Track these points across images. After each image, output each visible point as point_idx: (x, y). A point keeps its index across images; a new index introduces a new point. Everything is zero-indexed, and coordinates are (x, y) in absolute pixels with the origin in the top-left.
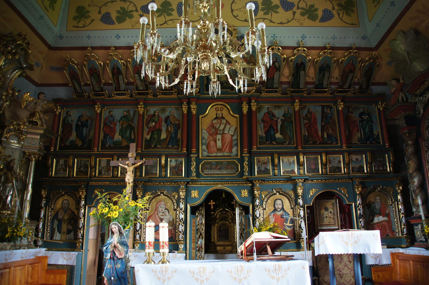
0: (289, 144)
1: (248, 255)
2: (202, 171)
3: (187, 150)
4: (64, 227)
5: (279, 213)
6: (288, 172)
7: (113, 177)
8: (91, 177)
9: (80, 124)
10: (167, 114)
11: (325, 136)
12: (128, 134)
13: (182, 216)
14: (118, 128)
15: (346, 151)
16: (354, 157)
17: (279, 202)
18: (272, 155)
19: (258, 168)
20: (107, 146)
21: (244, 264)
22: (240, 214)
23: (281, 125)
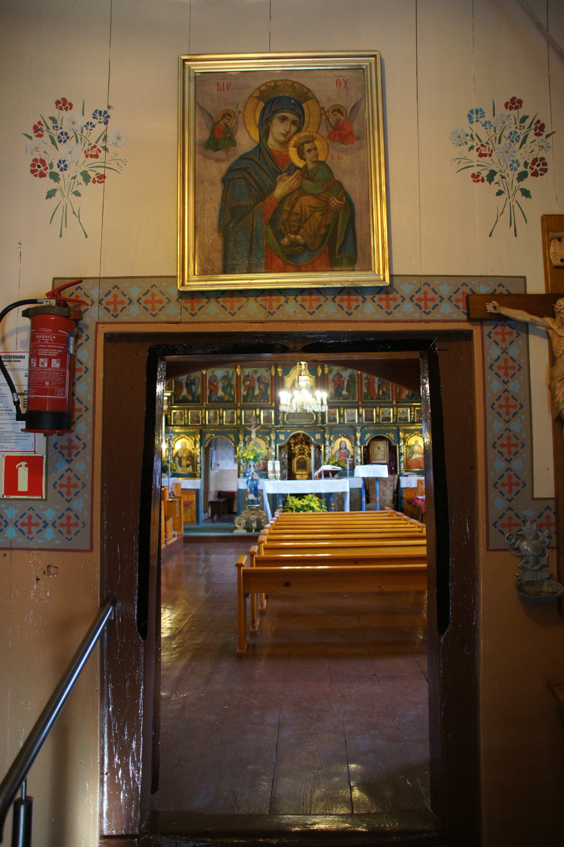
0: (353, 399)
1: (320, 476)
2: (287, 420)
3: (275, 404)
4: (184, 462)
5: (343, 451)
6: (350, 421)
7: (220, 424)
8: (202, 425)
9: (189, 382)
10: (258, 375)
11: (381, 393)
12: (229, 391)
13: (274, 454)
14: (220, 386)
15: (395, 406)
16: (401, 410)
17: (343, 443)
18: (339, 408)
19: (329, 418)
20: (213, 400)
21: (317, 481)
22: (315, 451)
23: (348, 385)
